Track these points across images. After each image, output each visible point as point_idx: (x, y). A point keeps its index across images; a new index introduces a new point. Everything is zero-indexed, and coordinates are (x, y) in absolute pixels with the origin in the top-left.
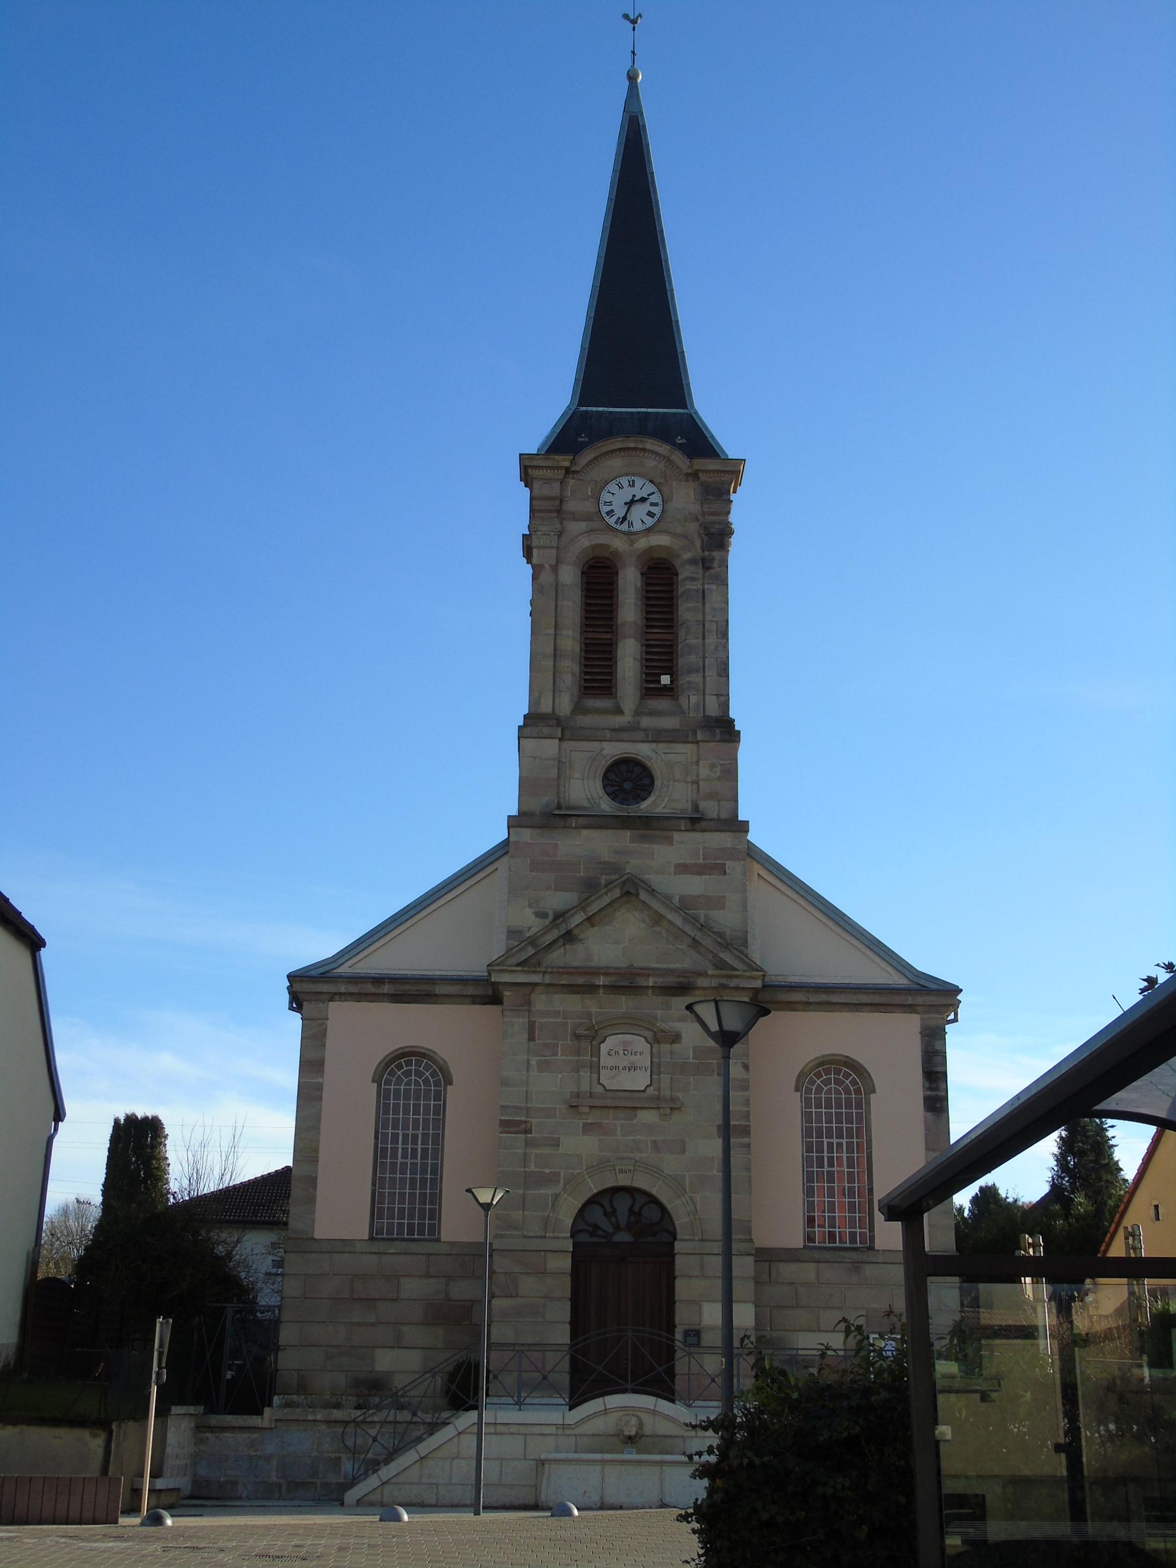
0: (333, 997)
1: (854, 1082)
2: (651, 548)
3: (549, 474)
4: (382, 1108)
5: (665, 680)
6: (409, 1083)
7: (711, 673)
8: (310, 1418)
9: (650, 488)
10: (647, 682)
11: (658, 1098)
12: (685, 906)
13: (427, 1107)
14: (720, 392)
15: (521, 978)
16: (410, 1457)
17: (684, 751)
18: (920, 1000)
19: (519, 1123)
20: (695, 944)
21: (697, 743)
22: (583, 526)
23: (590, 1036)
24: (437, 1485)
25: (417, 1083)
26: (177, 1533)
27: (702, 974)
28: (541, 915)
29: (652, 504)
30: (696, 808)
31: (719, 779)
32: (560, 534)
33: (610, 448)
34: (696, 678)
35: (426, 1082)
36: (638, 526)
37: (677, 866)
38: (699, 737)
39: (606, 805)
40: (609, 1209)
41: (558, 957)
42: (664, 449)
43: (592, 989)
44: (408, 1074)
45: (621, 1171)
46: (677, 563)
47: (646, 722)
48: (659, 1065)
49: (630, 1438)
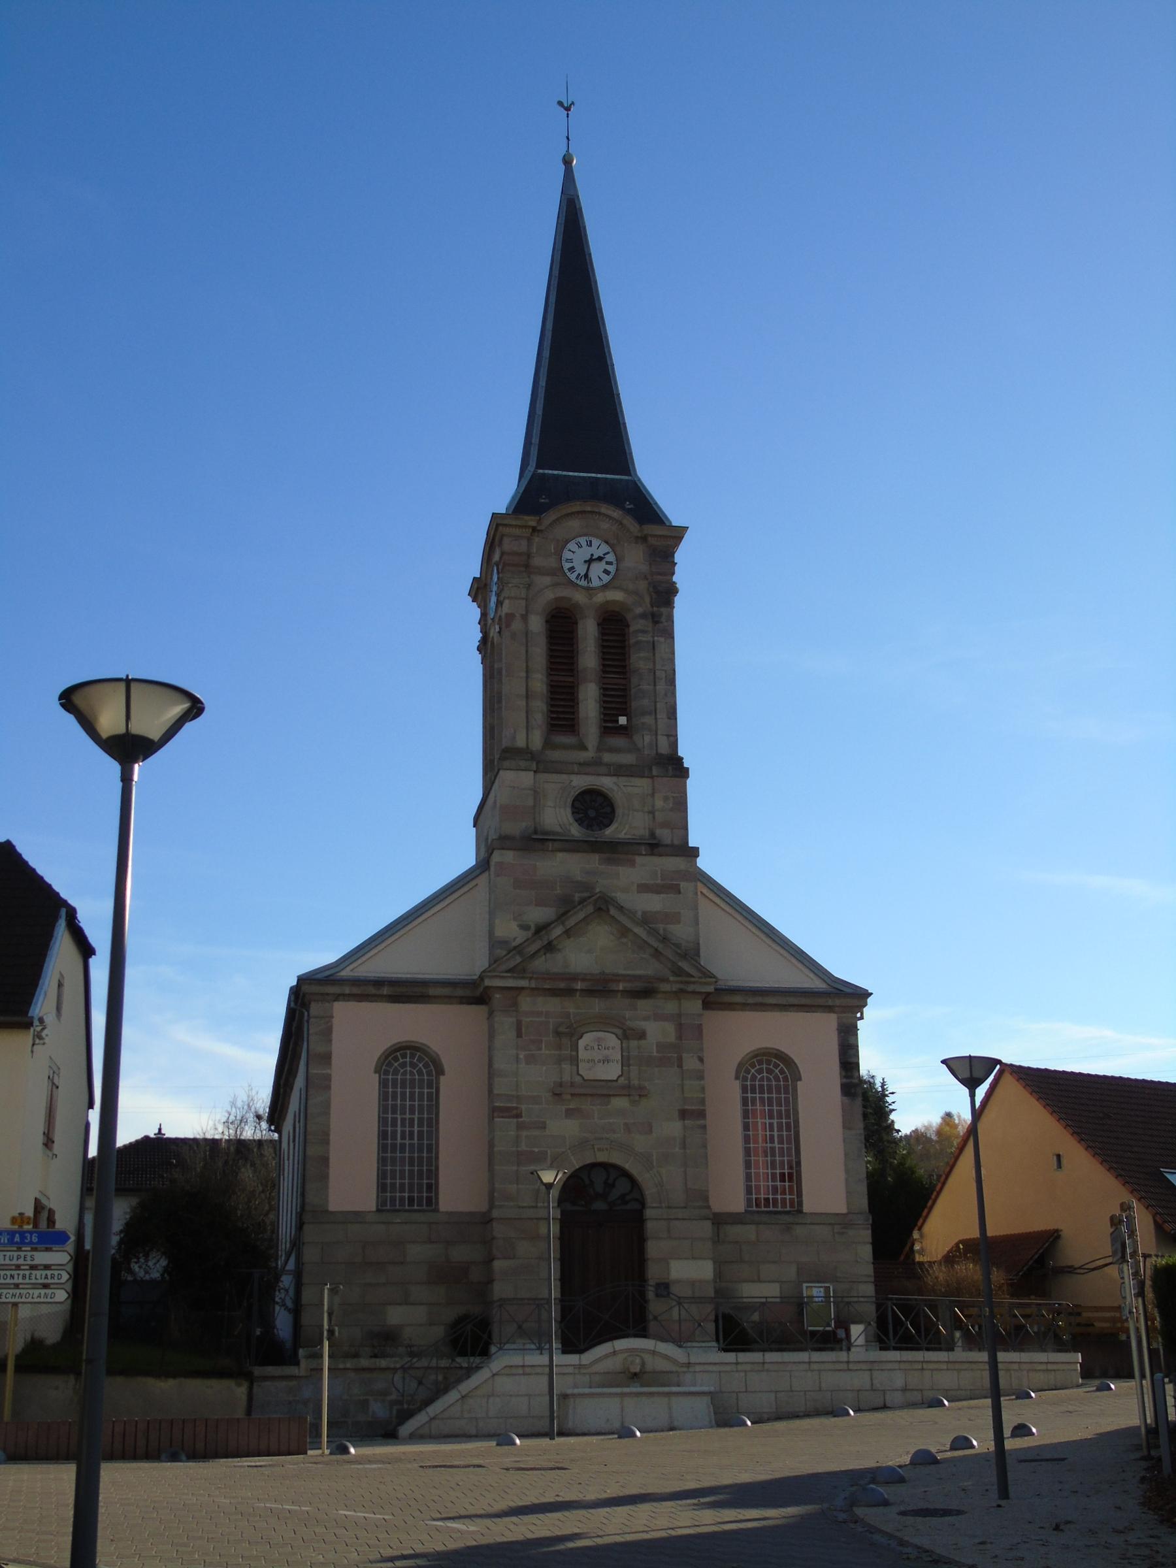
0: (338, 997)
1: (782, 1072)
2: (607, 602)
3: (517, 532)
4: (384, 1096)
5: (623, 720)
6: (405, 1073)
7: (662, 715)
8: (341, 1366)
9: (605, 548)
10: (605, 721)
11: (629, 1087)
12: (646, 920)
13: (421, 1094)
14: (660, 461)
15: (510, 983)
16: (453, 1396)
17: (640, 785)
18: (838, 1002)
19: (508, 1109)
20: (657, 954)
21: (652, 777)
22: (547, 580)
23: (568, 1033)
24: (476, 1419)
25: (412, 1073)
26: (358, 1460)
27: (666, 980)
28: (524, 927)
29: (607, 563)
30: (653, 835)
31: (671, 810)
32: (529, 586)
33: (574, 510)
34: (648, 720)
35: (420, 1073)
36: (596, 583)
37: (639, 886)
38: (655, 772)
39: (576, 831)
40: (610, 1181)
41: (540, 964)
42: (616, 514)
43: (569, 992)
44: (403, 1065)
45: (599, 1150)
46: (629, 617)
47: (607, 757)
48: (629, 1058)
49: (635, 1374)
